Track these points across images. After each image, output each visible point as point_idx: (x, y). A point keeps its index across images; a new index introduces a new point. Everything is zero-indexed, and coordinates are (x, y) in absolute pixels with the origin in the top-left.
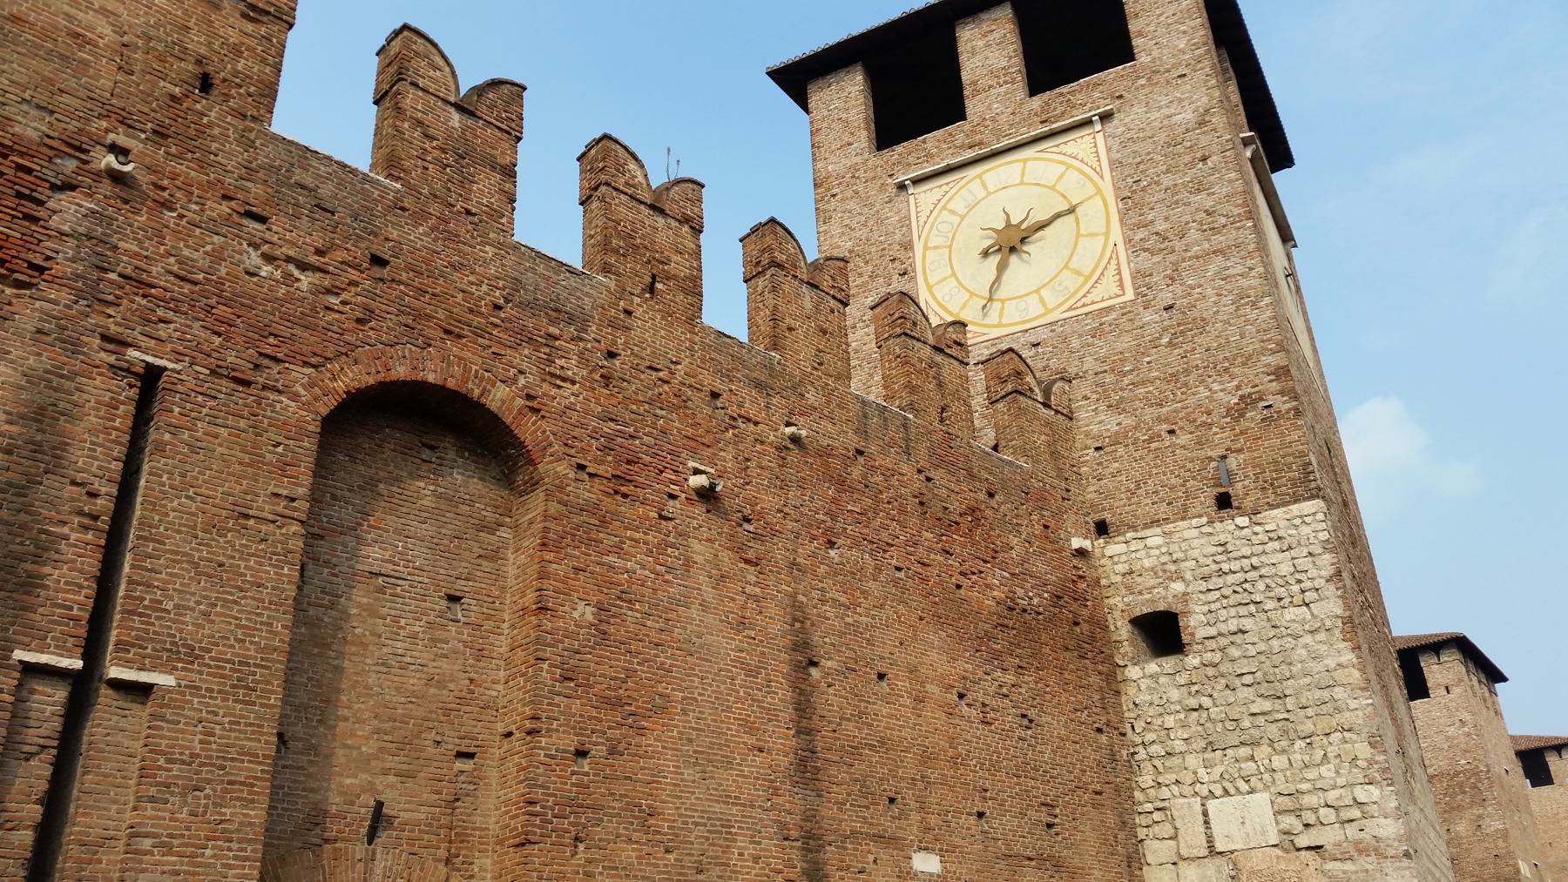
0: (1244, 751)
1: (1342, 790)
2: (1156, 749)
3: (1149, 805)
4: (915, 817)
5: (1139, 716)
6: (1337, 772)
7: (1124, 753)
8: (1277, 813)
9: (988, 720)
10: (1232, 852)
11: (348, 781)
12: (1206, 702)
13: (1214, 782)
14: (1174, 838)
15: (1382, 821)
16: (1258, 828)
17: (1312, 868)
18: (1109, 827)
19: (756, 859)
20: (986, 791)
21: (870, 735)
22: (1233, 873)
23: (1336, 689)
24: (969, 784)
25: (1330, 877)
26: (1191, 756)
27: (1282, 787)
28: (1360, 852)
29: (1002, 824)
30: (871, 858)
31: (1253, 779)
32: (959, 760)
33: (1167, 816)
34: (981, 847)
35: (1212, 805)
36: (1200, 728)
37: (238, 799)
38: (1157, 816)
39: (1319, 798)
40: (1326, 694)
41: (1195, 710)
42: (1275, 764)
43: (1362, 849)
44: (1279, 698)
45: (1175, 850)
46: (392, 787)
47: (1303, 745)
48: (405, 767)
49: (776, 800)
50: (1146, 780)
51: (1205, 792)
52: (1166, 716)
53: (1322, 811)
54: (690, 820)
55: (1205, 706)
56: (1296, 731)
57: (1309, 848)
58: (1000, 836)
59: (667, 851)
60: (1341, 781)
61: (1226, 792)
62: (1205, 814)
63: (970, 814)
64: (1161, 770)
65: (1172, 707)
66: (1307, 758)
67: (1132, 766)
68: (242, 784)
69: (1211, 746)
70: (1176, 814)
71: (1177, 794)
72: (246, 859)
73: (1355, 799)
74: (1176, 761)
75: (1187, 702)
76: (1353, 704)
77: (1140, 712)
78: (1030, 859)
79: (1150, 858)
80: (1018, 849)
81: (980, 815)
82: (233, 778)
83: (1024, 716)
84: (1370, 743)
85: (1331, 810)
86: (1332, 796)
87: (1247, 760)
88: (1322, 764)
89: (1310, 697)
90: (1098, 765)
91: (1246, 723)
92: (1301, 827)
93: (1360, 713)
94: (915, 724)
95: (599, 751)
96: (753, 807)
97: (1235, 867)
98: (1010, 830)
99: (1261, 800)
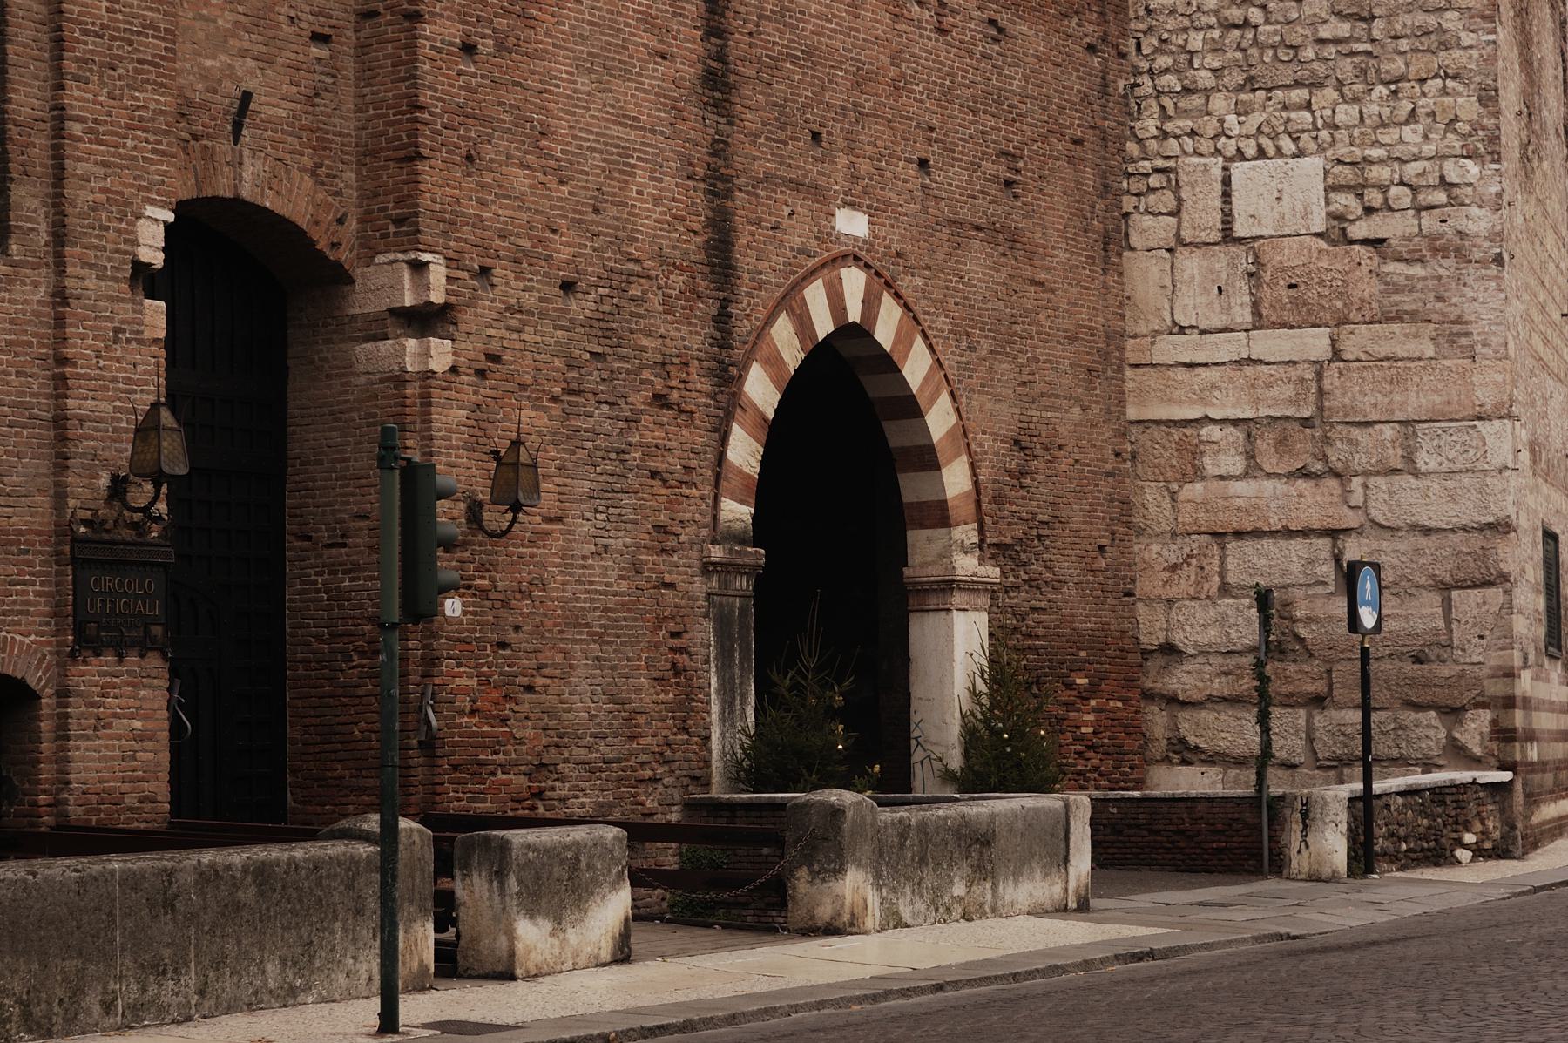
0: (1298, 95)
1: (1427, 164)
2: (1170, 81)
3: (1147, 164)
4: (843, 160)
5: (1151, 29)
6: (1426, 137)
7: (1121, 83)
8: (1330, 189)
9: (945, 26)
10: (1255, 238)
11: (209, 63)
12: (1255, 15)
13: (1248, 137)
14: (1176, 213)
15: (1474, 210)
16: (1299, 207)
17: (1364, 269)
18: (1085, 192)
19: (657, 201)
20: (932, 129)
21: (794, 41)
22: (1252, 269)
23: (1448, 15)
24: (911, 119)
25: (1387, 283)
26: (1219, 95)
27: (1342, 151)
28: (1435, 251)
29: (950, 177)
30: (787, 211)
31: (1305, 137)
32: (902, 84)
33: (1169, 181)
34: (919, 206)
35: (1239, 170)
36: (1239, 55)
37: (147, 81)
38: (1154, 181)
39: (1393, 171)
40: (1432, 20)
41: (1236, 26)
42: (1340, 118)
43: (1438, 245)
44: (1363, 19)
45: (1174, 231)
46: (251, 73)
47: (1385, 92)
48: (263, 49)
49: (681, 126)
50: (1149, 126)
51: (1231, 150)
52: (1192, 34)
53: (1394, 191)
54: (586, 144)
55: (1253, 21)
56: (1378, 71)
57: (1365, 242)
58: (944, 195)
59: (562, 183)
60: (1429, 149)
61: (1261, 154)
62: (1227, 182)
63: (909, 161)
64: (1171, 112)
65: (1204, 19)
66: (1386, 112)
67: (1130, 107)
68: (150, 63)
69: (1250, 84)
70: (1183, 178)
71: (1189, 149)
72: (163, 153)
73: (1442, 178)
74: (1197, 101)
75: (1227, 13)
76: (1467, 39)
77: (1154, 23)
78: (978, 228)
79: (1135, 240)
80: (965, 213)
81: (923, 163)
82: (141, 56)
83: (992, 22)
84: (1480, 100)
85: (1407, 191)
86: (1412, 169)
87: (1300, 107)
88: (1407, 123)
89: (1409, 23)
90: (1082, 100)
91: (1309, 53)
92: (1359, 211)
93: (1475, 53)
94: (851, 29)
95: (486, 46)
96: (653, 132)
97: (1257, 262)
98: (957, 186)
99: (1313, 165)
